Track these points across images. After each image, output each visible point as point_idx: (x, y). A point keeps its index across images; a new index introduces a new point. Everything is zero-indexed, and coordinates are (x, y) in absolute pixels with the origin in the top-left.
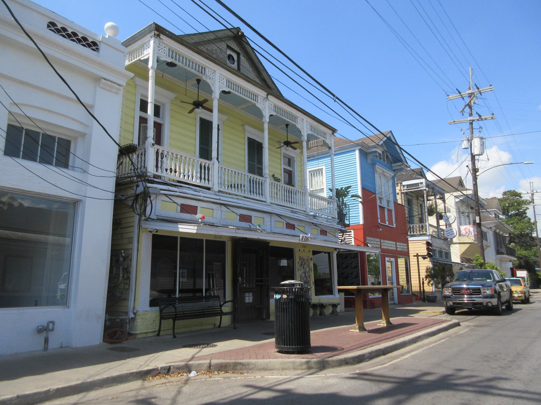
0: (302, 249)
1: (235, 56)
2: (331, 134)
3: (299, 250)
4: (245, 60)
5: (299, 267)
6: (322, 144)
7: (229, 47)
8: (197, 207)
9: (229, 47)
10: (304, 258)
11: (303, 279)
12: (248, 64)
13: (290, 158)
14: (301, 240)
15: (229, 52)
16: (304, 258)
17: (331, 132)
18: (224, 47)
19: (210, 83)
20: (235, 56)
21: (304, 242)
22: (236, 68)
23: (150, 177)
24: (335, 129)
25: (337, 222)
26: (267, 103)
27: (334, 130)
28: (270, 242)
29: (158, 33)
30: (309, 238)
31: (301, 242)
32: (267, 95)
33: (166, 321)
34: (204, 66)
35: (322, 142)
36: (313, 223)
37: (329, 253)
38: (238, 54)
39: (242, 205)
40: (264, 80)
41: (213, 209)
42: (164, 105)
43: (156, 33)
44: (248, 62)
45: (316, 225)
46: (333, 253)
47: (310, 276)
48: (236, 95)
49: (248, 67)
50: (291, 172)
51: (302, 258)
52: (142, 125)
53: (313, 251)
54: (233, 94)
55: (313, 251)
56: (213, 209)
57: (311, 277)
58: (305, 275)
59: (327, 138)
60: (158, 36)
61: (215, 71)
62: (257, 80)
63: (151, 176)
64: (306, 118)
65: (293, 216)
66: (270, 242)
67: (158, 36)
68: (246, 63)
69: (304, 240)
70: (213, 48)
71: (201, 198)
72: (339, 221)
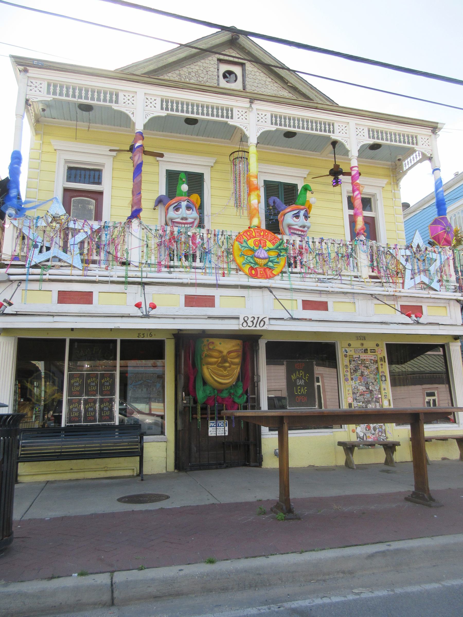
0: (356, 344)
1: (237, 70)
2: (431, 134)
3: (349, 345)
4: (256, 70)
5: (349, 374)
6: (421, 157)
7: (220, 60)
8: (92, 292)
9: (220, 60)
10: (361, 358)
11: (361, 395)
12: (262, 74)
13: (369, 197)
14: (241, 323)
15: (224, 68)
16: (361, 358)
17: (428, 131)
18: (212, 63)
19: (127, 112)
20: (237, 70)
21: (253, 328)
22: (240, 87)
23: (4, 260)
24: (438, 123)
25: (453, 287)
26: (252, 116)
27: (435, 125)
28: (261, 336)
29: (23, 67)
30: (266, 320)
31: (243, 328)
32: (251, 102)
33: (22, 463)
34: (195, 102)
35: (420, 154)
36: (372, 295)
37: (443, 346)
38: (242, 65)
39: (185, 281)
40: (294, 89)
41: (126, 293)
42: (103, 165)
43: (21, 68)
44: (263, 72)
45: (375, 298)
46: (448, 344)
47: (380, 389)
48: (208, 121)
49: (264, 79)
50: (373, 219)
51: (359, 358)
52: (73, 199)
53: (387, 344)
54: (203, 120)
55: (387, 344)
56: (126, 293)
57: (383, 392)
58: (369, 389)
59: (420, 142)
60: (26, 71)
61: (136, 92)
62: (285, 93)
63: (6, 259)
64: (353, 121)
65: (317, 286)
66: (261, 336)
67: (26, 71)
68: (258, 74)
69: (250, 324)
70: (190, 70)
71: (97, 279)
72: (458, 285)
